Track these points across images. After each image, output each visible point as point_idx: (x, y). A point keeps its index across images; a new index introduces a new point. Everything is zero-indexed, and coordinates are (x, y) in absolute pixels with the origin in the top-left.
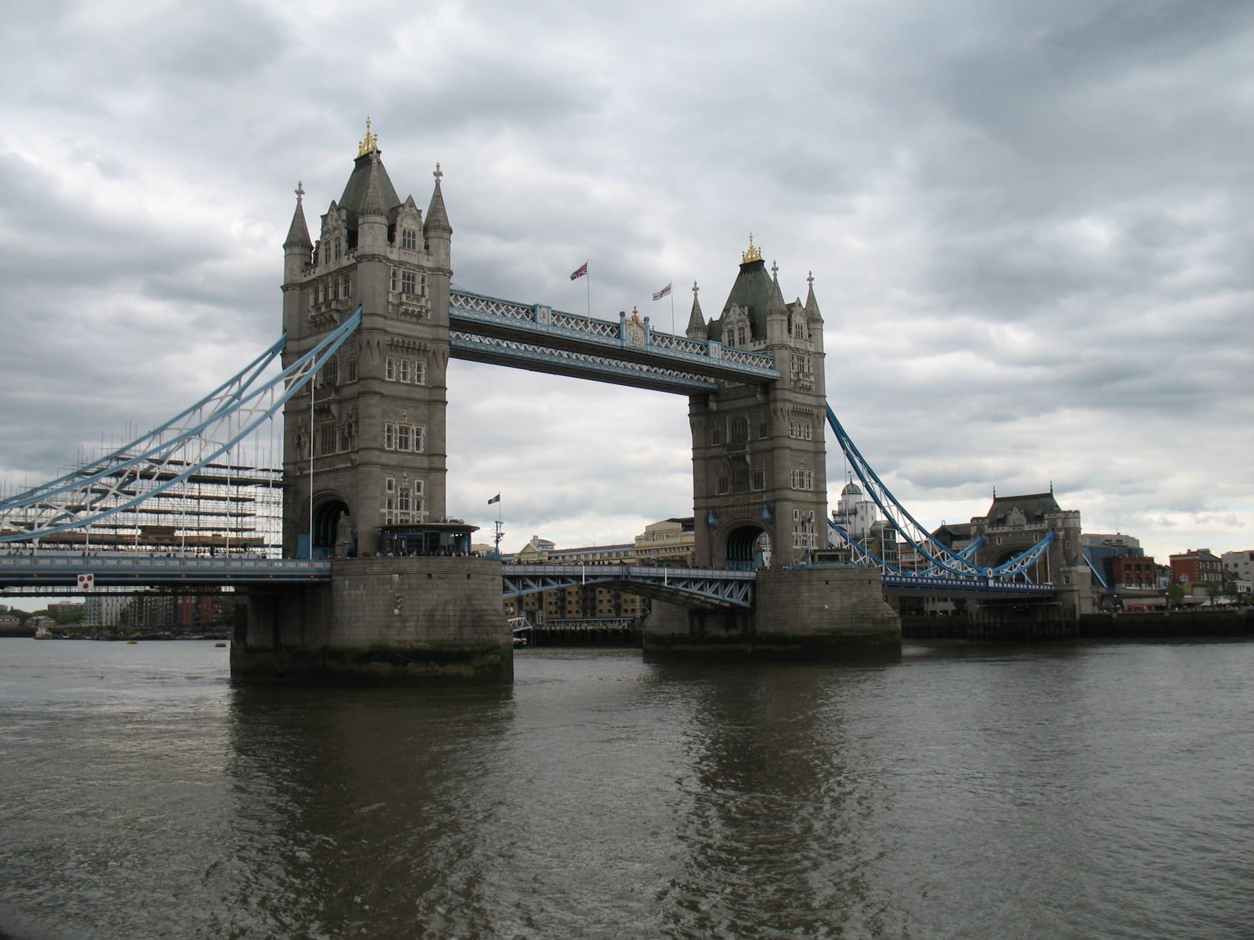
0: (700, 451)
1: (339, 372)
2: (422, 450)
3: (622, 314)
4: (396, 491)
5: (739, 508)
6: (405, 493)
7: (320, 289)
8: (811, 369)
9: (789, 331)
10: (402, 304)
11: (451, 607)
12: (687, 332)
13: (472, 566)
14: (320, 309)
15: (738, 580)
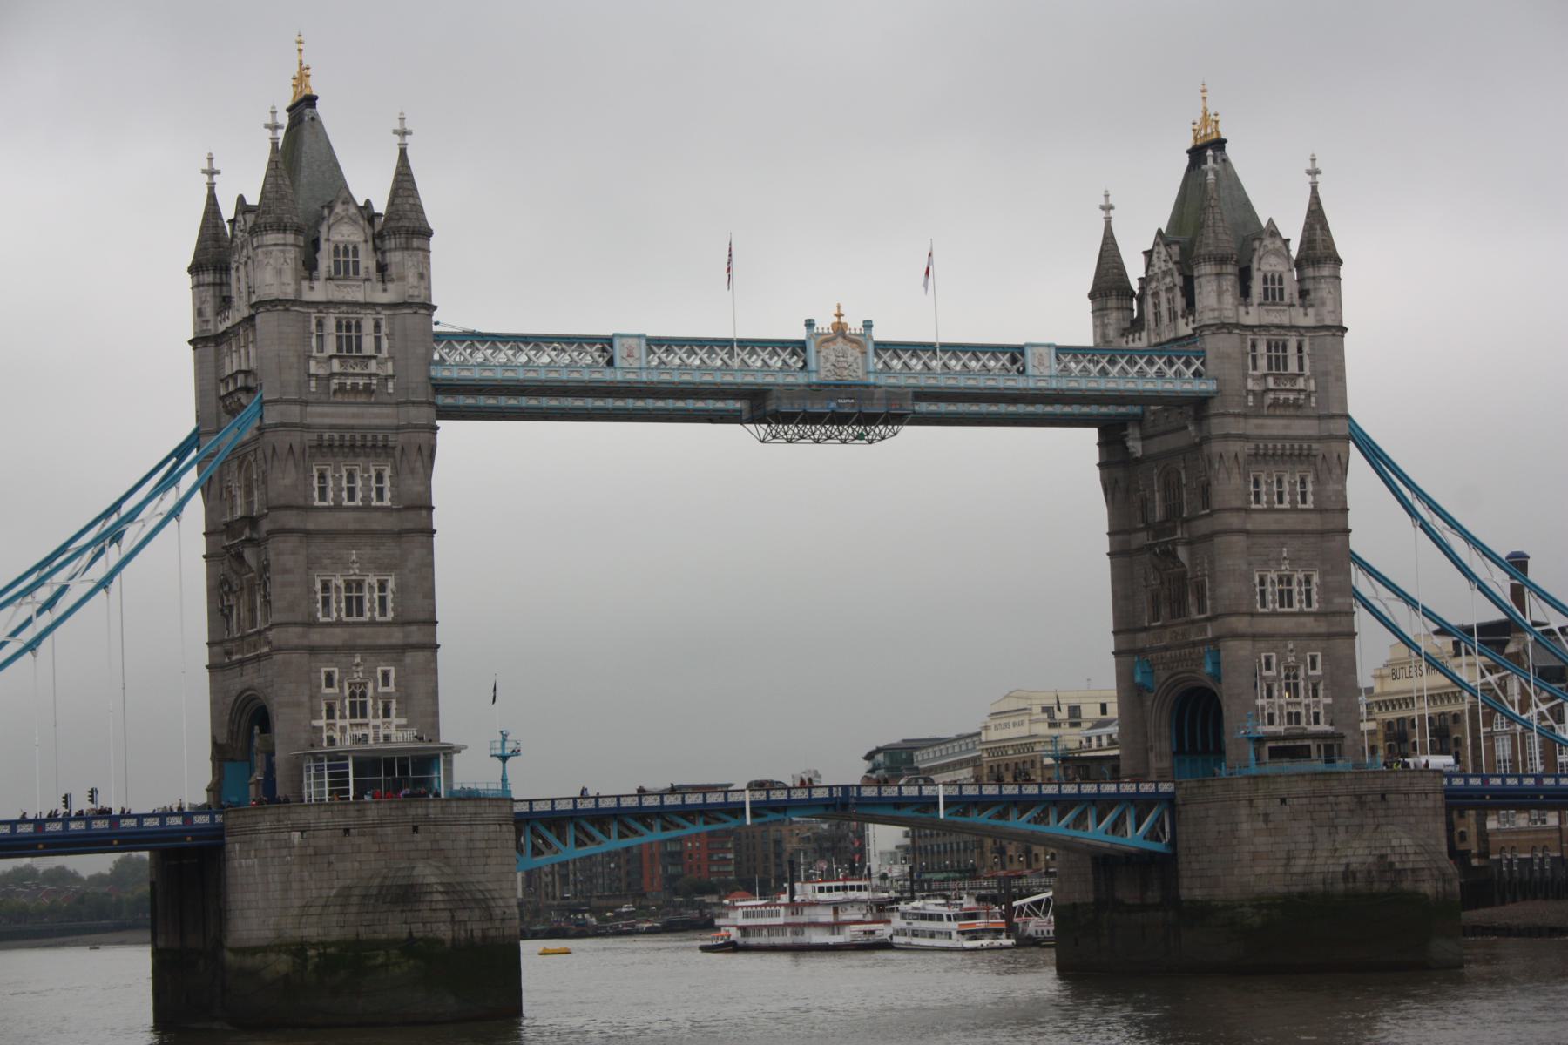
0: (1119, 538)
1: (256, 493)
2: (390, 615)
3: (810, 324)
4: (341, 689)
5: (1178, 652)
6: (358, 692)
7: (234, 349)
8: (1307, 362)
9: (1245, 292)
10: (333, 375)
11: (377, 882)
12: (1092, 296)
13: (420, 811)
14: (227, 385)
15: (1132, 801)
